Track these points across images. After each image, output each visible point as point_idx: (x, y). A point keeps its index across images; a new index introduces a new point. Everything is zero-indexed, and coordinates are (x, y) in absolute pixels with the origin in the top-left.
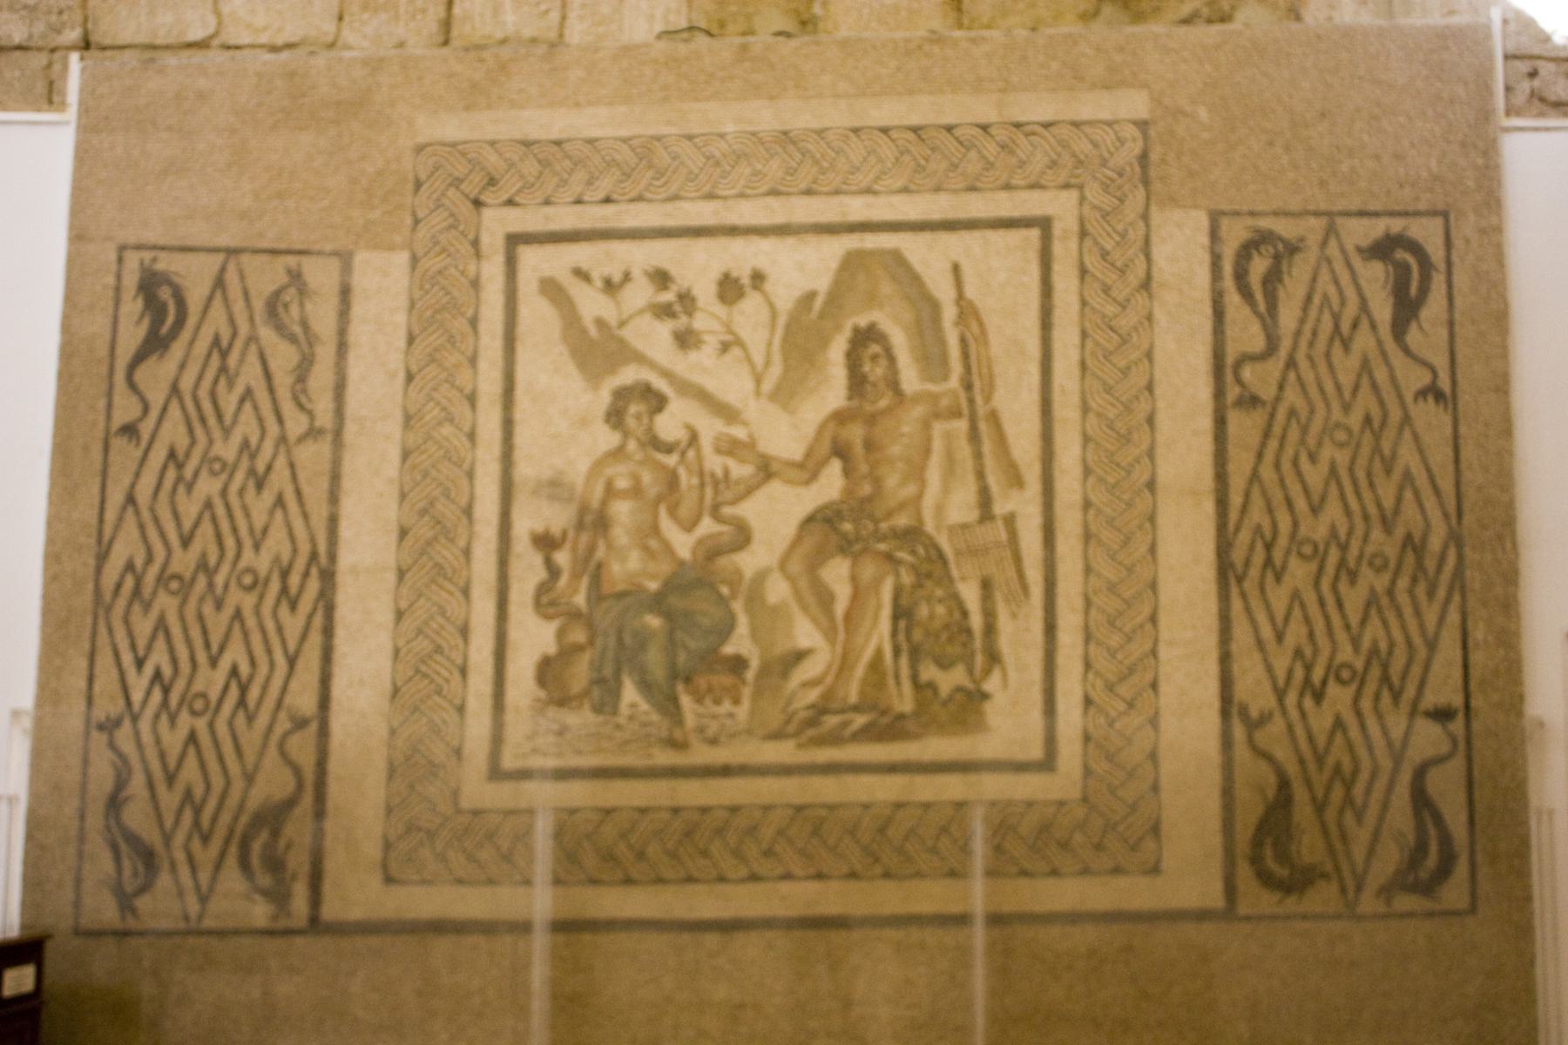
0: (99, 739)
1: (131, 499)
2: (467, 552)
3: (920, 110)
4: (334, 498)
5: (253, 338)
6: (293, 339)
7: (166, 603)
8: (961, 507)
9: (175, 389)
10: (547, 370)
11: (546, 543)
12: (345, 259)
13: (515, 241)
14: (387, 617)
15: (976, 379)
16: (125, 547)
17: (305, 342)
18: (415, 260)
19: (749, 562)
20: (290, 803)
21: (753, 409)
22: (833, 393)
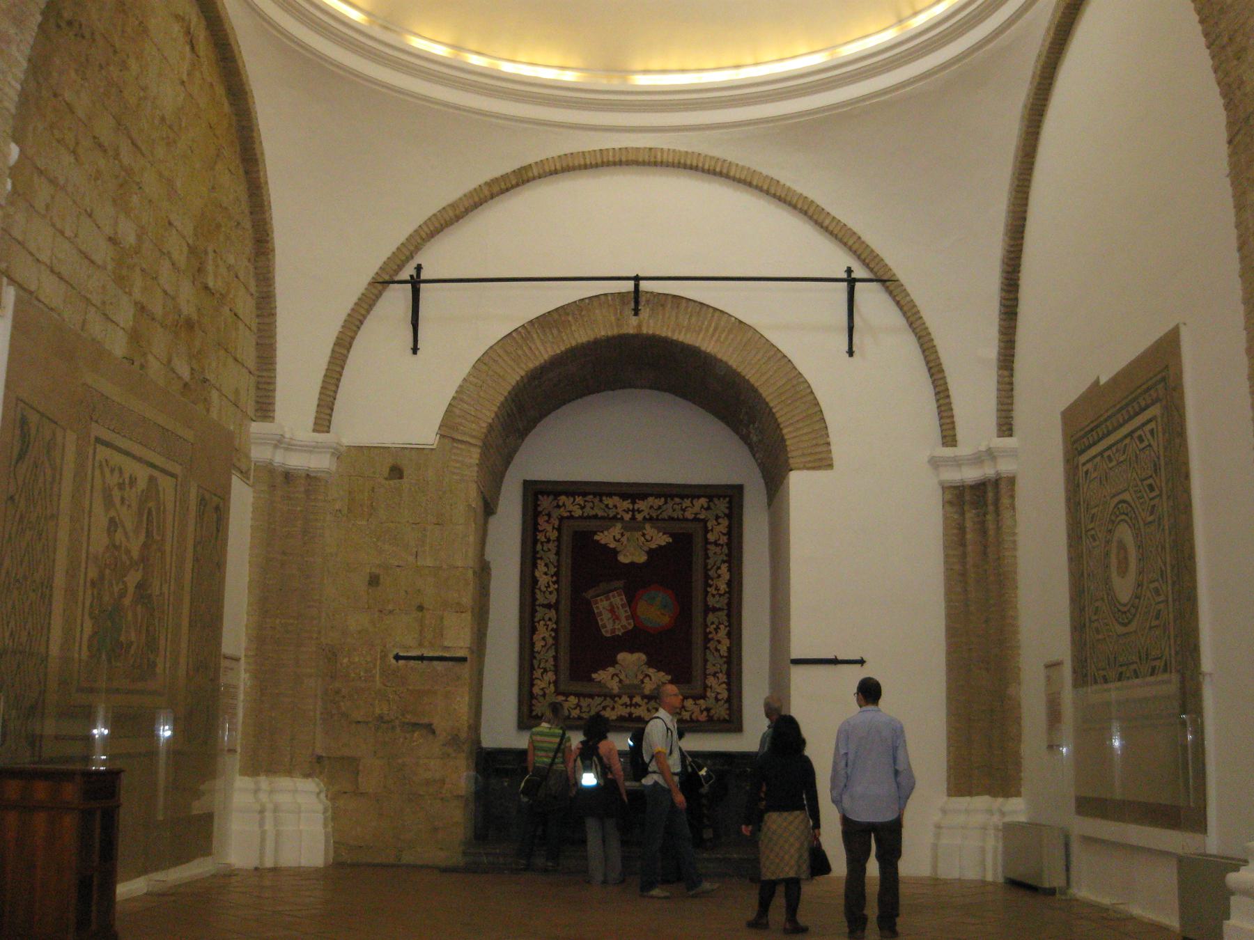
11: (93, 584)
12: (65, 430)
13: (98, 440)
18: (78, 439)
19: (127, 601)
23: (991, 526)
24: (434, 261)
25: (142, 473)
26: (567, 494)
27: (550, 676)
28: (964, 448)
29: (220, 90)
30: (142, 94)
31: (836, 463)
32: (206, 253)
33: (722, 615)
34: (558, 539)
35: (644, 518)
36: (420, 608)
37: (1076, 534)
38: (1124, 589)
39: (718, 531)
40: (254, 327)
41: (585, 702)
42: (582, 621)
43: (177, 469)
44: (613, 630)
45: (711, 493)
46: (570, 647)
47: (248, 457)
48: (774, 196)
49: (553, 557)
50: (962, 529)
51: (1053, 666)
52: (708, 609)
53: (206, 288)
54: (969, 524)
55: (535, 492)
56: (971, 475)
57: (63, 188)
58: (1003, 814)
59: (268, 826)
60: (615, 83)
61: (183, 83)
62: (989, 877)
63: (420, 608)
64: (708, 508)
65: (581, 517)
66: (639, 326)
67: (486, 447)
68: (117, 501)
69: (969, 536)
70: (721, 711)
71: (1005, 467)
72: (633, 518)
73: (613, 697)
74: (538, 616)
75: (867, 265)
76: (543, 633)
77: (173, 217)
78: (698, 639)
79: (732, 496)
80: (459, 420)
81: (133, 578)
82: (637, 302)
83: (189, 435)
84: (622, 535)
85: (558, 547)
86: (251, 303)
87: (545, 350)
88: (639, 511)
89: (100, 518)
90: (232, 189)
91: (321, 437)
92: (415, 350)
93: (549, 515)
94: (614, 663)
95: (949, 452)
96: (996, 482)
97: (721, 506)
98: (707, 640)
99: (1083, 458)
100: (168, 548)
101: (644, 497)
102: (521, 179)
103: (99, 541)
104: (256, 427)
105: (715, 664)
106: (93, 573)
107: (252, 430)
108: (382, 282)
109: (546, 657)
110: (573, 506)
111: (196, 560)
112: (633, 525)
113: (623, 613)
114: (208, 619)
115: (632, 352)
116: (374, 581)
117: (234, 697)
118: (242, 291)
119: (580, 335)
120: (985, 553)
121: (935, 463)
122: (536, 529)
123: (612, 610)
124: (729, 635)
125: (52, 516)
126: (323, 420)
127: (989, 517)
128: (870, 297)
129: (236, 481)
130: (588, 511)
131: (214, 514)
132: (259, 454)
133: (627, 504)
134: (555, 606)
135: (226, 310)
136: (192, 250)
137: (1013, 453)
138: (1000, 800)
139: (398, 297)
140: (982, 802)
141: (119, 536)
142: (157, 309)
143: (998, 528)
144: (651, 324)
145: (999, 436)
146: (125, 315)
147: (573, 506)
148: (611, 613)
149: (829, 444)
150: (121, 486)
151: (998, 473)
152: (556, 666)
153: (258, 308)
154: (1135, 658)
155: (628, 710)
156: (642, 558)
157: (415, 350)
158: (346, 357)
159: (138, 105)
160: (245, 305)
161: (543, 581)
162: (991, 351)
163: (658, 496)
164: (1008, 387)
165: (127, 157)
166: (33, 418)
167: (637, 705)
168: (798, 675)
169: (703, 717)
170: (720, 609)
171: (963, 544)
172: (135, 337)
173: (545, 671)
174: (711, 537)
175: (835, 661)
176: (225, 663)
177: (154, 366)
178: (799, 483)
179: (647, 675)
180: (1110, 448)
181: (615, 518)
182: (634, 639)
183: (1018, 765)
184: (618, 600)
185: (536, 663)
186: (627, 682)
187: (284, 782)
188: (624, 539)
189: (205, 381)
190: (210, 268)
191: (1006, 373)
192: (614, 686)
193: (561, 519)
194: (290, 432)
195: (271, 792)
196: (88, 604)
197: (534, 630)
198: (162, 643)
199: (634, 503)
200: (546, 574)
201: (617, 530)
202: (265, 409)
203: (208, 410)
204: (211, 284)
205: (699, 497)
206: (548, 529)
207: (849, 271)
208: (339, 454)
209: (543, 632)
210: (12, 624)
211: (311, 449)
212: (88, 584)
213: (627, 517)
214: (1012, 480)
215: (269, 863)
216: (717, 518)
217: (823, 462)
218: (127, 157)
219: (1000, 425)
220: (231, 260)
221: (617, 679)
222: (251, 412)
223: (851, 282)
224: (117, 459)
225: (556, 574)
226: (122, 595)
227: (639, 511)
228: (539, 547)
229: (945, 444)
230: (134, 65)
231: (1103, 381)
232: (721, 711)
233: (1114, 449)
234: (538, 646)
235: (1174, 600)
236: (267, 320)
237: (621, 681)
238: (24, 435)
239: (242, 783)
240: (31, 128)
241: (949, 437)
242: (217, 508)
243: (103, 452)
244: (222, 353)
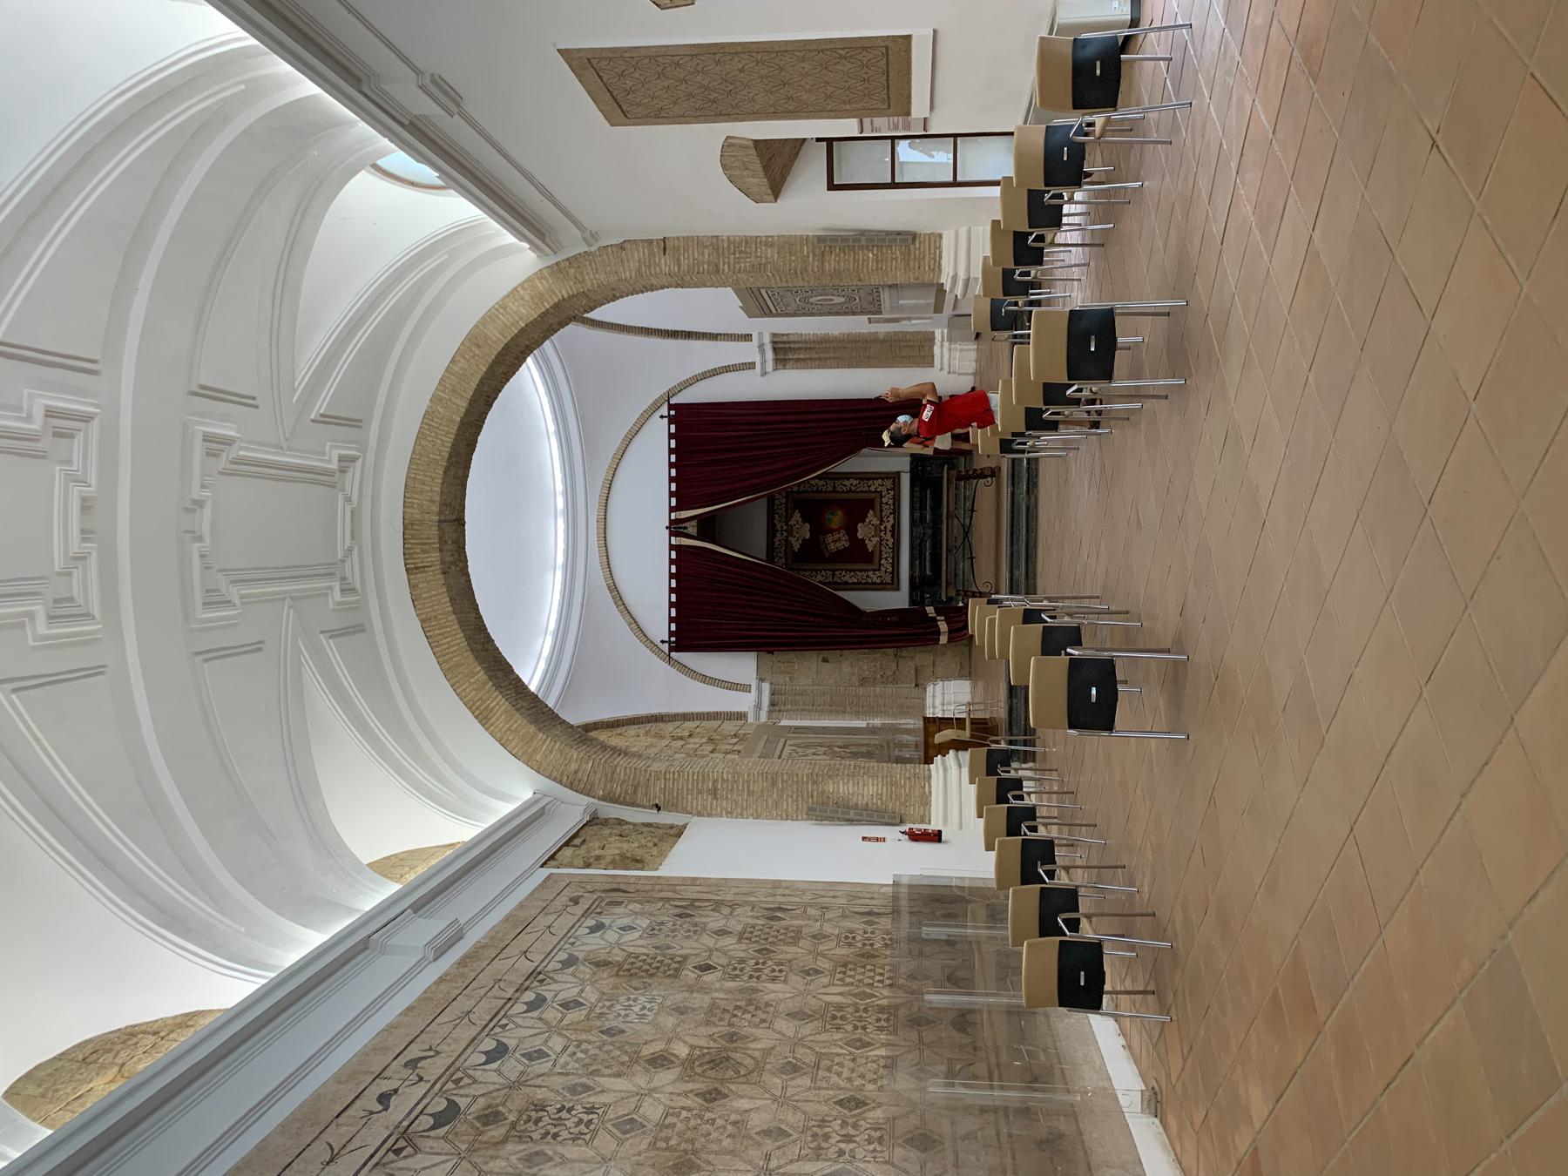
3: (762, 744)
28: (757, 359)
37: (812, 314)
42: (842, 557)
50: (798, 360)
51: (870, 321)
52: (834, 491)
56: (770, 355)
70: (889, 483)
71: (767, 340)
78: (850, 496)
91: (754, 687)
95: (758, 366)
102: (614, 589)
104: (751, 720)
105: (863, 487)
112: (790, 531)
113: (836, 536)
126: (746, 688)
132: (764, 718)
137: (760, 334)
140: (936, 349)
148: (837, 542)
156: (807, 526)
171: (805, 360)
182: (852, 532)
183: (917, 333)
184: (830, 538)
201: (792, 540)
202: (741, 716)
208: (761, 680)
211: (760, 690)
214: (774, 335)
232: (889, 483)
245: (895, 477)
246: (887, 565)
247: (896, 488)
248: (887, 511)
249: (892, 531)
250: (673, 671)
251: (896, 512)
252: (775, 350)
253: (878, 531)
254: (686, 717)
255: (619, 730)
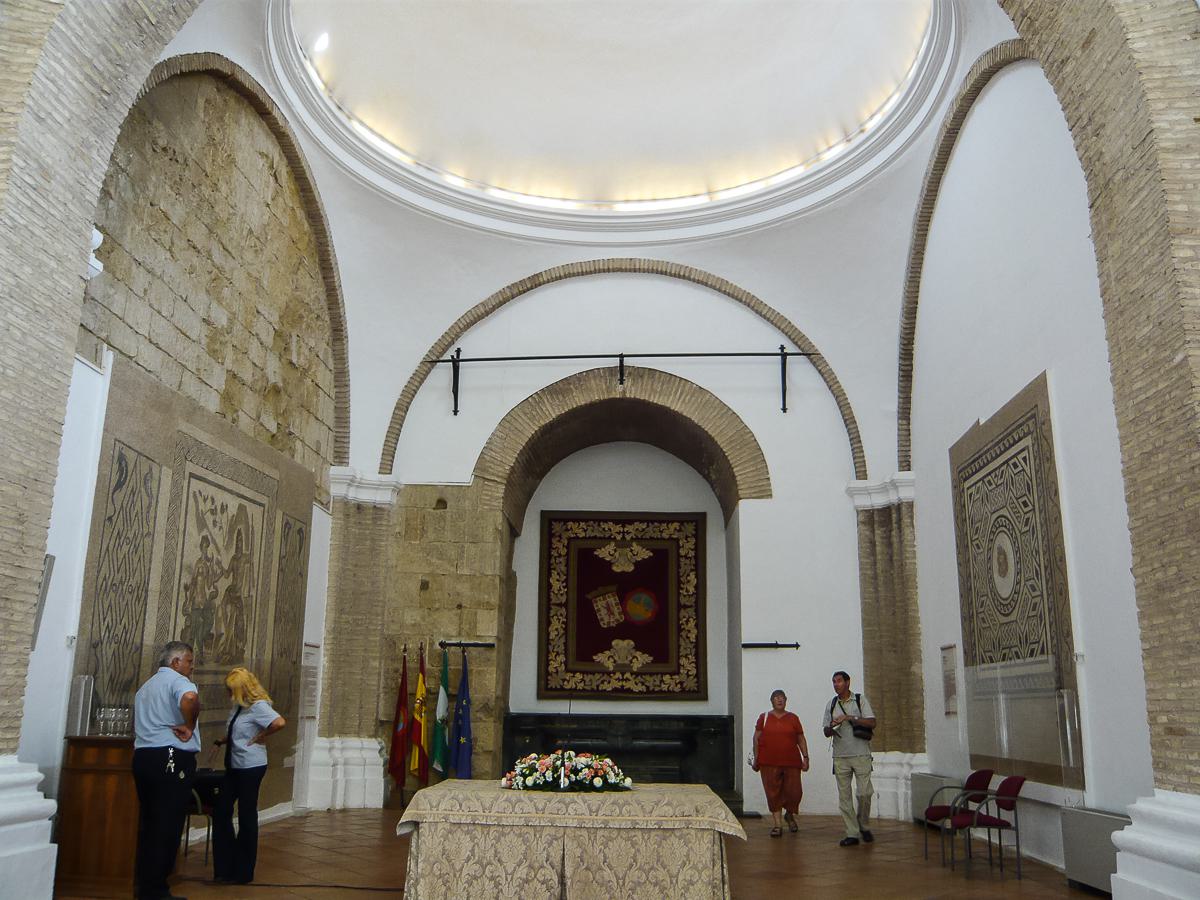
0: (93, 650)
1: (107, 549)
2: (172, 587)
3: (250, 461)
4: (150, 562)
5: (140, 491)
6: (148, 496)
7: (112, 594)
8: (246, 595)
9: (122, 506)
10: (192, 527)
11: (186, 588)
12: (161, 466)
13: (192, 475)
14: (156, 610)
15: (252, 554)
16: (104, 570)
17: (150, 496)
19: (218, 601)
20: (131, 681)
21: (223, 551)
22: (233, 552)
23: (895, 540)
24: (471, 344)
25: (233, 504)
26: (574, 521)
27: (562, 658)
29: (300, 214)
30: (231, 211)
31: (774, 494)
32: (291, 336)
33: (691, 611)
34: (567, 554)
35: (632, 538)
36: (460, 607)
37: (963, 546)
38: (1004, 586)
39: (687, 548)
40: (333, 395)
41: (588, 678)
42: (585, 615)
43: (264, 500)
44: (609, 623)
45: (682, 518)
46: (577, 640)
47: (328, 493)
48: (725, 292)
49: (563, 568)
50: (873, 544)
52: (680, 607)
53: (291, 363)
54: (878, 539)
55: (549, 519)
56: (879, 501)
57: (160, 277)
58: (911, 766)
59: (340, 776)
60: (604, 211)
61: (268, 205)
62: (902, 817)
63: (460, 607)
64: (680, 531)
65: (584, 538)
66: (624, 392)
67: (510, 483)
68: (210, 523)
69: (878, 549)
70: (691, 684)
71: (905, 494)
72: (624, 538)
73: (609, 673)
74: (552, 613)
75: (796, 343)
76: (556, 625)
77: (260, 308)
78: (673, 630)
79: (698, 521)
80: (488, 464)
81: (223, 584)
82: (622, 375)
83: (275, 474)
84: (615, 551)
85: (567, 560)
86: (330, 377)
87: (553, 411)
88: (628, 533)
89: (194, 537)
90: (313, 291)
91: (385, 478)
92: (456, 412)
93: (560, 536)
94: (609, 647)
95: (861, 483)
96: (899, 507)
97: (690, 528)
98: (680, 629)
99: (967, 484)
100: (256, 560)
101: (631, 522)
102: (534, 283)
103: (193, 555)
104: (335, 471)
106: (186, 579)
107: (331, 472)
108: (431, 362)
109: (558, 644)
110: (578, 530)
111: (281, 570)
112: (623, 544)
113: (616, 610)
114: (291, 615)
115: (616, 415)
116: (424, 586)
117: (315, 675)
118: (322, 367)
119: (580, 399)
120: (891, 560)
121: (851, 493)
122: (550, 547)
123: (608, 608)
124: (696, 626)
125: (148, 534)
126: (387, 466)
127: (894, 533)
128: (799, 368)
129: (317, 510)
130: (590, 533)
131: (297, 537)
132: (336, 490)
133: (619, 528)
134: (565, 605)
135: (308, 381)
136: (278, 334)
137: (911, 483)
138: (909, 755)
139: (443, 372)
141: (211, 550)
142: (247, 377)
143: (901, 542)
144: (632, 390)
145: (900, 471)
146: (218, 379)
147: (578, 530)
148: (607, 610)
149: (768, 479)
150: (213, 512)
151: (899, 499)
152: (566, 650)
153: (336, 381)
154: (1015, 642)
155: (620, 684)
157: (456, 412)
158: (404, 418)
159: (228, 219)
160: (325, 378)
161: (556, 585)
162: (893, 405)
163: (641, 521)
164: (907, 433)
165: (218, 256)
166: (131, 456)
167: (627, 680)
168: (747, 656)
169: (678, 689)
170: (691, 607)
171: (873, 553)
172: (227, 397)
173: (558, 654)
174: (682, 552)
175: (776, 646)
176: (305, 650)
177: (245, 422)
178: (746, 508)
179: (634, 657)
180: (989, 474)
181: (610, 538)
182: (624, 630)
184: (612, 600)
185: (551, 648)
186: (619, 662)
187: (353, 741)
188: (617, 554)
189: (290, 434)
190: (294, 347)
191: (904, 422)
192: (610, 665)
193: (569, 539)
194: (360, 475)
195: (343, 749)
196: (181, 604)
197: (549, 623)
198: (249, 635)
199: (623, 527)
200: (558, 580)
201: (611, 547)
202: (341, 457)
203: (293, 456)
204: (294, 361)
205: (673, 522)
206: (560, 547)
207: (782, 348)
208: (398, 490)
209: (556, 625)
210: (108, 619)
211: (378, 487)
212: (182, 588)
213: (619, 537)
214: (911, 505)
215: (339, 805)
216: (687, 537)
217: (764, 492)
218: (218, 256)
219: (900, 462)
220: (312, 343)
221: (612, 660)
222: (330, 459)
223: (784, 356)
224: (211, 491)
225: (566, 581)
226: (214, 596)
227: (628, 533)
228: (553, 560)
229: (858, 478)
230: (224, 188)
231: (982, 422)
232: (691, 684)
233: (993, 475)
234: (553, 635)
235: (1048, 595)
236: (343, 390)
237: (615, 662)
238: (122, 470)
239: (320, 742)
240: (129, 228)
241: (861, 473)
242: (300, 531)
243: (196, 485)
244: (305, 413)
245: (700, 693)
246: (575, 681)
247: (685, 695)
248: (650, 681)
249: (622, 690)
250: (413, 364)
251: (650, 695)
252: (886, 511)
253: (623, 669)
254: (341, 377)
255: (311, 263)
